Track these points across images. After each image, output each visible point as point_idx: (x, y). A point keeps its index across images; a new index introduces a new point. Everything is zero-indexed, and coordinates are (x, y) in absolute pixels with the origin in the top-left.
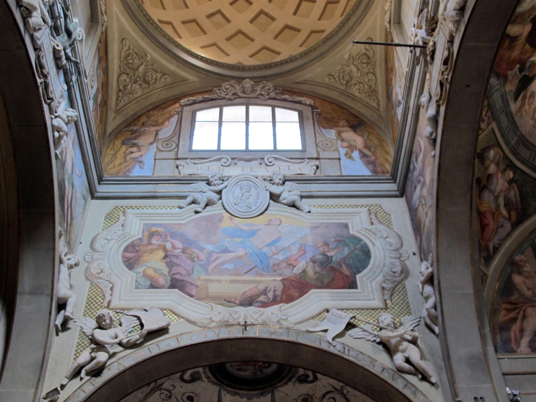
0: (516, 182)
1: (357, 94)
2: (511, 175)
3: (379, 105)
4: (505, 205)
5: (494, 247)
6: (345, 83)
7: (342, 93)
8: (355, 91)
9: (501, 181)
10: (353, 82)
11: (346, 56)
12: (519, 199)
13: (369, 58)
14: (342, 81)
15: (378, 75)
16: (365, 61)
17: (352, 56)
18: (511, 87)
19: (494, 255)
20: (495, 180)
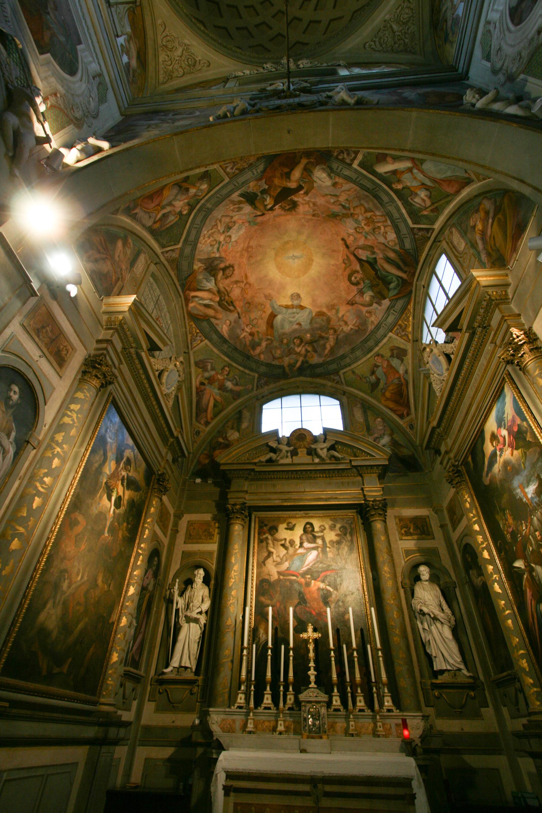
0: (180, 218)
1: (161, 59)
2: (185, 212)
3: (164, 83)
4: (164, 215)
5: (136, 214)
6: (164, 44)
7: (155, 41)
8: (162, 57)
9: (181, 203)
10: (169, 53)
11: (186, 42)
12: (168, 226)
13: (194, 66)
14: (164, 40)
15: (185, 78)
16: (190, 63)
17: (189, 47)
18: (252, 187)
19: (130, 216)
20: (184, 197)
